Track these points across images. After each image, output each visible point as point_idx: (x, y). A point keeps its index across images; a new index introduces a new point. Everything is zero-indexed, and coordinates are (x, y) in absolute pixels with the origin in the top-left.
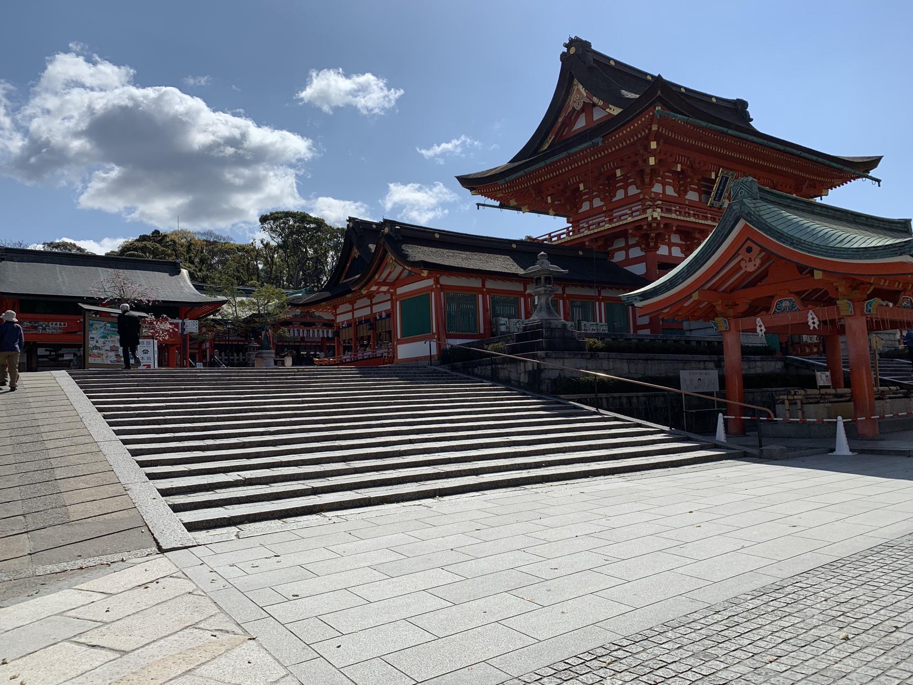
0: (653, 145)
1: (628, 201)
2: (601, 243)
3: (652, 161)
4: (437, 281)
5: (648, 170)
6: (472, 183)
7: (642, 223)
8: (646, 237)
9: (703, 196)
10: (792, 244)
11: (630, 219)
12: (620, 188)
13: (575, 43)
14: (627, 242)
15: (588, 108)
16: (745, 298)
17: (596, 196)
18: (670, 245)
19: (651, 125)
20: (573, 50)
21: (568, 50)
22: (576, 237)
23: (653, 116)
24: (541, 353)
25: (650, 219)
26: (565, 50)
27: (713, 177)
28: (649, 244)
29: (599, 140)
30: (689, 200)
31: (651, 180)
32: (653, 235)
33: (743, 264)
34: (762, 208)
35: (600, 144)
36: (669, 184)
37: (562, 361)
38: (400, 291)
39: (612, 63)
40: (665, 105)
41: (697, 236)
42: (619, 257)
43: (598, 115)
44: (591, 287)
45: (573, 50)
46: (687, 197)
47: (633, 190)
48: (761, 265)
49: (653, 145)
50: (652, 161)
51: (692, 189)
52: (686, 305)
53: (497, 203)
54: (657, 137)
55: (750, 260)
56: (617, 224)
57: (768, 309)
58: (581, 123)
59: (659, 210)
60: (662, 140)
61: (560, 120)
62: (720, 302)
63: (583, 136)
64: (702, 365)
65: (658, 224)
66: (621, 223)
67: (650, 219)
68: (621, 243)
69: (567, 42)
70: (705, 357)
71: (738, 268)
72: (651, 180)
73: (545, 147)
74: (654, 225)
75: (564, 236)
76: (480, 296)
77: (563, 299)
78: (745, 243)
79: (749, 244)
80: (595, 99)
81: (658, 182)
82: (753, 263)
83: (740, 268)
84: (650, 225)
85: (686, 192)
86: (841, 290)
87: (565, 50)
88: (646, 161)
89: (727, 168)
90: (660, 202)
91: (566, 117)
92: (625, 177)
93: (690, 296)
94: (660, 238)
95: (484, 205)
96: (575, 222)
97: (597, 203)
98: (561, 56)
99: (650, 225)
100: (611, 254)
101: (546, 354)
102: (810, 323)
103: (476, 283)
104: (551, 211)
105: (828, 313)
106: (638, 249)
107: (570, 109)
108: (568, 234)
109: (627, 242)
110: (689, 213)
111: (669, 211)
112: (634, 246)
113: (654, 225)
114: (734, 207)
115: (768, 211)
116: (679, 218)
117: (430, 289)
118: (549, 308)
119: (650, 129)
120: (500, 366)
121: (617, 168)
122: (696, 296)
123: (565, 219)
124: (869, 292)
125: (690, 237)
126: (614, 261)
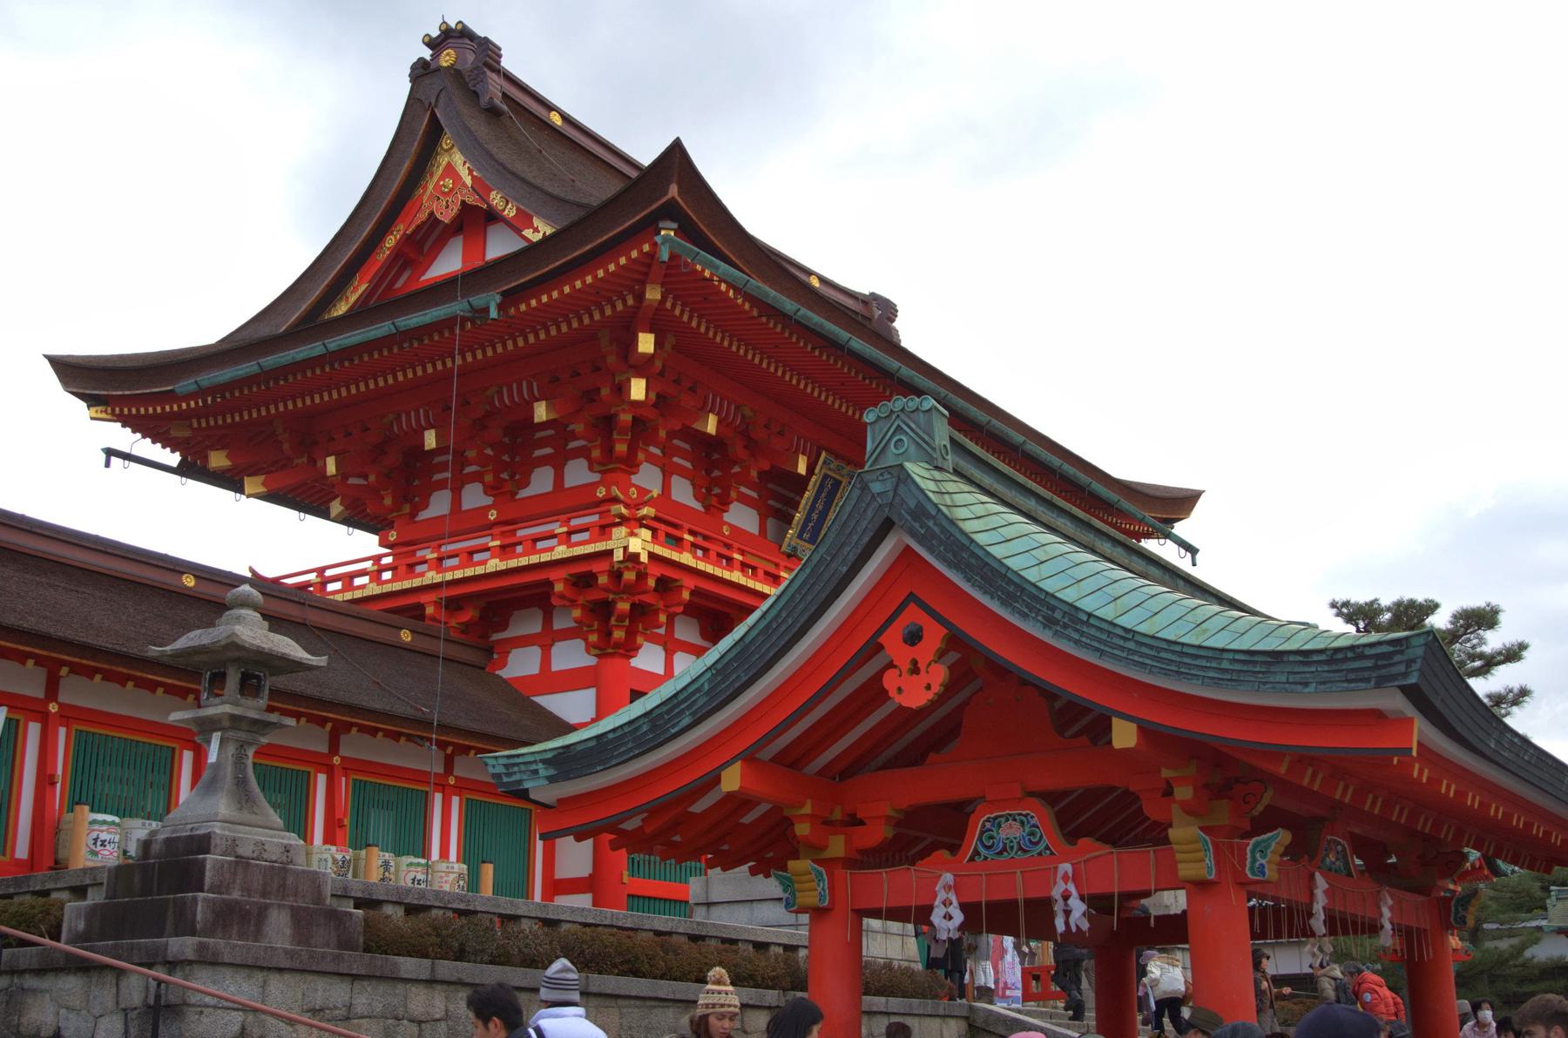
0: (646, 343)
2: (469, 614)
3: (638, 389)
6: (100, 382)
7: (595, 567)
8: (602, 610)
9: (770, 522)
10: (1050, 622)
11: (561, 552)
12: (544, 461)
13: (453, 36)
14: (548, 621)
15: (474, 220)
16: (886, 801)
17: (476, 477)
19: (643, 284)
20: (447, 58)
21: (435, 57)
22: (397, 586)
23: (652, 256)
25: (618, 555)
26: (427, 54)
27: (802, 469)
28: (610, 634)
31: (633, 450)
32: (624, 606)
33: (890, 681)
34: (959, 499)
35: (493, 314)
36: (683, 472)
37: (260, 976)
39: (556, 119)
40: (688, 231)
42: (522, 664)
43: (499, 246)
45: (447, 58)
46: (727, 517)
47: (578, 474)
48: (950, 688)
49: (646, 343)
50: (638, 389)
51: (744, 500)
53: (174, 459)
55: (915, 670)
56: (524, 561)
58: (449, 263)
59: (646, 534)
60: (671, 340)
61: (391, 242)
62: (807, 809)
63: (446, 288)
65: (642, 576)
66: (534, 559)
67: (618, 555)
68: (528, 624)
69: (435, 33)
72: (633, 450)
73: (341, 309)
74: (630, 576)
75: (364, 580)
77: (330, 771)
79: (913, 616)
80: (496, 199)
81: (651, 459)
82: (923, 678)
83: (883, 696)
84: (616, 575)
85: (724, 503)
86: (1183, 793)
87: (427, 54)
88: (622, 389)
89: (837, 457)
91: (407, 240)
94: (641, 617)
96: (405, 553)
98: (414, 67)
99: (616, 575)
100: (492, 653)
101: (202, 948)
104: (336, 507)
106: (579, 644)
107: (422, 216)
108: (376, 576)
109: (548, 621)
110: (730, 560)
111: (678, 543)
112: (567, 635)
113: (630, 576)
114: (876, 487)
115: (979, 510)
116: (701, 566)
118: (241, 782)
119: (640, 297)
120: (30, 982)
122: (732, 780)
123: (375, 539)
124: (1260, 808)
126: (505, 673)
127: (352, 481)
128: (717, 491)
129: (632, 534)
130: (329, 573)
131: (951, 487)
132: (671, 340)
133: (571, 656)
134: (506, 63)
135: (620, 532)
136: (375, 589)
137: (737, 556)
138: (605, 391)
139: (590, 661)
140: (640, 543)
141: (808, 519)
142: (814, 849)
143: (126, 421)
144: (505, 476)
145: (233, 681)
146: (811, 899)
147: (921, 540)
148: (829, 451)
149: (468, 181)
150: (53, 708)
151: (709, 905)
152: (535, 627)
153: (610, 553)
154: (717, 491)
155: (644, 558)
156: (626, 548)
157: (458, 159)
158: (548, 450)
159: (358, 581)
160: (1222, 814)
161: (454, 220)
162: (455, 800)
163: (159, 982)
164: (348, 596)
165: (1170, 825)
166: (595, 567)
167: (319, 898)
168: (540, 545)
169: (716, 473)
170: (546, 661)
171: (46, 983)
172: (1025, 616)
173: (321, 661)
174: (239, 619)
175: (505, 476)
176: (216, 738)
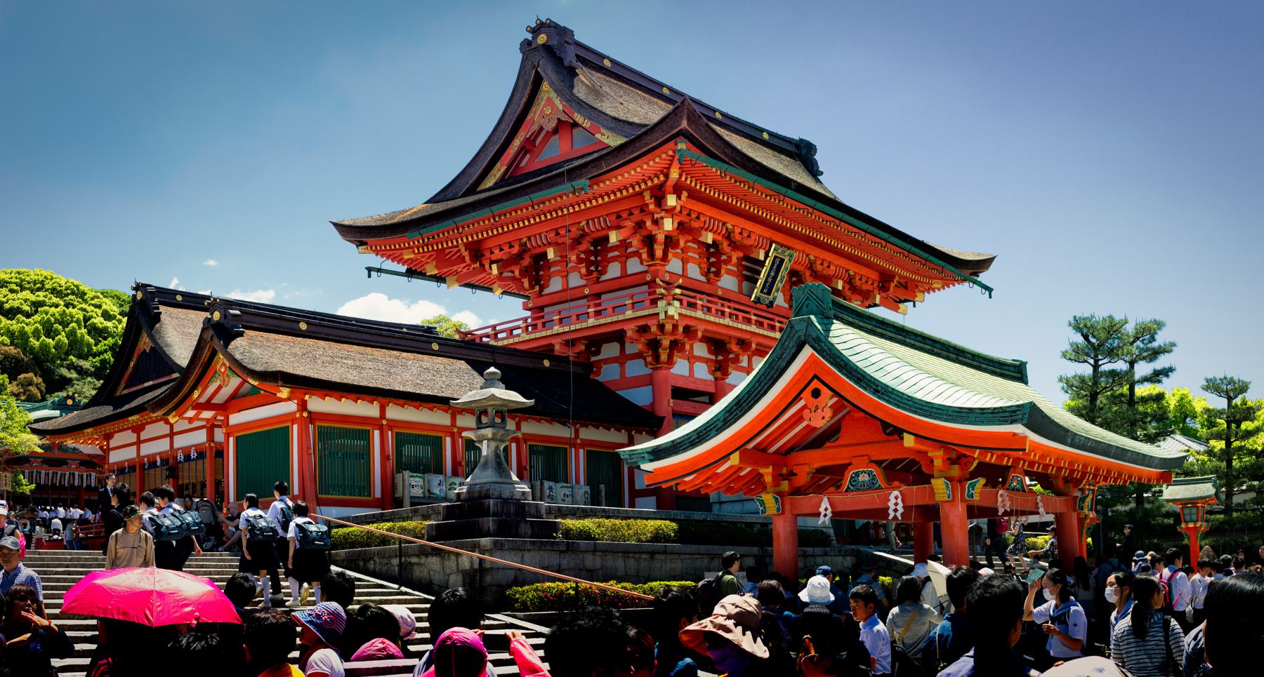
0: (671, 201)
1: (625, 283)
3: (668, 225)
4: (303, 406)
5: (661, 237)
8: (654, 345)
9: (745, 284)
10: (876, 392)
15: (565, 126)
18: (692, 359)
19: (668, 169)
22: (538, 335)
24: (485, 541)
25: (662, 316)
27: (762, 257)
29: (584, 182)
30: (723, 289)
32: (666, 343)
33: (806, 413)
38: (236, 419)
41: (734, 347)
44: (564, 424)
46: (719, 284)
50: (668, 225)
51: (729, 272)
52: (719, 471)
57: (837, 485)
59: (677, 303)
60: (685, 194)
65: (675, 327)
66: (615, 319)
67: (662, 316)
71: (798, 418)
74: (669, 327)
78: (811, 381)
81: (676, 255)
84: (661, 327)
90: (678, 291)
92: (624, 244)
93: (726, 457)
94: (676, 346)
95: (379, 270)
97: (575, 280)
101: (495, 543)
102: (892, 507)
103: (367, 409)
105: (917, 494)
106: (641, 361)
110: (723, 313)
111: (692, 306)
113: (669, 327)
117: (290, 418)
119: (667, 176)
120: (414, 560)
125: (723, 352)
127: (505, 275)
128: (713, 269)
129: (669, 304)
132: (685, 194)
134: (578, 37)
135: (661, 304)
136: (525, 337)
137: (727, 310)
138: (649, 223)
139: (648, 371)
140: (674, 310)
141: (766, 282)
144: (592, 268)
148: (777, 243)
150: (384, 422)
154: (713, 269)
155: (676, 317)
158: (617, 253)
159: (515, 332)
160: (955, 471)
162: (581, 451)
163: (481, 560)
164: (511, 341)
165: (933, 476)
169: (712, 260)
172: (865, 389)
173: (531, 402)
175: (592, 268)
176: (485, 442)
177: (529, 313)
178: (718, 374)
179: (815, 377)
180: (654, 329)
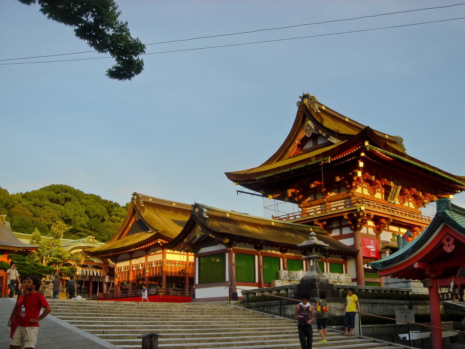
8: (355, 222)
14: (341, 223)
26: (300, 100)
31: (356, 184)
32: (360, 220)
36: (365, 187)
49: (361, 164)
51: (379, 192)
54: (363, 159)
55: (449, 246)
62: (428, 269)
64: (402, 307)
65: (364, 214)
67: (359, 210)
70: (403, 302)
76: (256, 257)
79: (448, 236)
80: (320, 132)
84: (358, 214)
85: (375, 193)
87: (300, 100)
113: (361, 214)
118: (317, 269)
121: (337, 176)
122: (416, 265)
130: (290, 215)
131: (453, 214)
133: (346, 231)
139: (352, 232)
142: (428, 276)
143: (241, 185)
145: (314, 251)
146: (430, 285)
147: (448, 224)
149: (313, 128)
151: (387, 284)
152: (338, 225)
153: (356, 210)
156: (360, 209)
157: (310, 123)
161: (311, 137)
166: (354, 213)
167: (334, 289)
168: (339, 208)
170: (341, 232)
171: (289, 306)
174: (313, 239)
176: (311, 261)
177: (300, 210)
178: (378, 232)
179: (447, 233)
180: (355, 215)
